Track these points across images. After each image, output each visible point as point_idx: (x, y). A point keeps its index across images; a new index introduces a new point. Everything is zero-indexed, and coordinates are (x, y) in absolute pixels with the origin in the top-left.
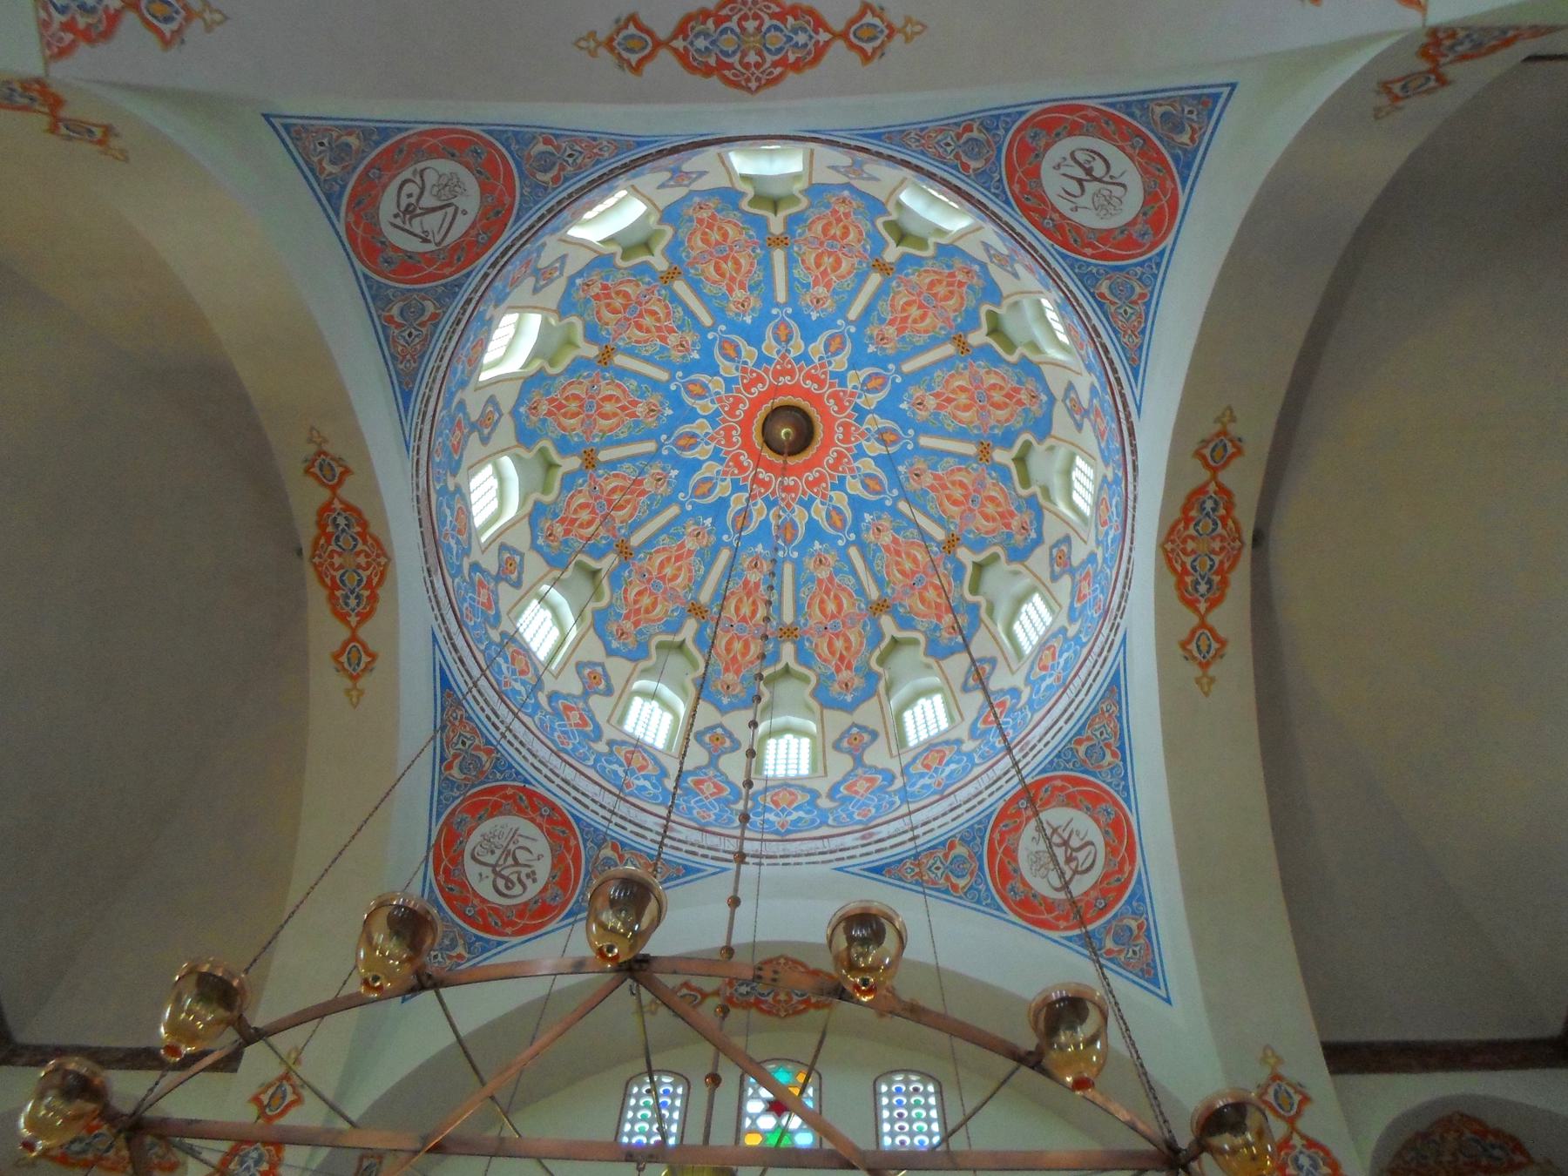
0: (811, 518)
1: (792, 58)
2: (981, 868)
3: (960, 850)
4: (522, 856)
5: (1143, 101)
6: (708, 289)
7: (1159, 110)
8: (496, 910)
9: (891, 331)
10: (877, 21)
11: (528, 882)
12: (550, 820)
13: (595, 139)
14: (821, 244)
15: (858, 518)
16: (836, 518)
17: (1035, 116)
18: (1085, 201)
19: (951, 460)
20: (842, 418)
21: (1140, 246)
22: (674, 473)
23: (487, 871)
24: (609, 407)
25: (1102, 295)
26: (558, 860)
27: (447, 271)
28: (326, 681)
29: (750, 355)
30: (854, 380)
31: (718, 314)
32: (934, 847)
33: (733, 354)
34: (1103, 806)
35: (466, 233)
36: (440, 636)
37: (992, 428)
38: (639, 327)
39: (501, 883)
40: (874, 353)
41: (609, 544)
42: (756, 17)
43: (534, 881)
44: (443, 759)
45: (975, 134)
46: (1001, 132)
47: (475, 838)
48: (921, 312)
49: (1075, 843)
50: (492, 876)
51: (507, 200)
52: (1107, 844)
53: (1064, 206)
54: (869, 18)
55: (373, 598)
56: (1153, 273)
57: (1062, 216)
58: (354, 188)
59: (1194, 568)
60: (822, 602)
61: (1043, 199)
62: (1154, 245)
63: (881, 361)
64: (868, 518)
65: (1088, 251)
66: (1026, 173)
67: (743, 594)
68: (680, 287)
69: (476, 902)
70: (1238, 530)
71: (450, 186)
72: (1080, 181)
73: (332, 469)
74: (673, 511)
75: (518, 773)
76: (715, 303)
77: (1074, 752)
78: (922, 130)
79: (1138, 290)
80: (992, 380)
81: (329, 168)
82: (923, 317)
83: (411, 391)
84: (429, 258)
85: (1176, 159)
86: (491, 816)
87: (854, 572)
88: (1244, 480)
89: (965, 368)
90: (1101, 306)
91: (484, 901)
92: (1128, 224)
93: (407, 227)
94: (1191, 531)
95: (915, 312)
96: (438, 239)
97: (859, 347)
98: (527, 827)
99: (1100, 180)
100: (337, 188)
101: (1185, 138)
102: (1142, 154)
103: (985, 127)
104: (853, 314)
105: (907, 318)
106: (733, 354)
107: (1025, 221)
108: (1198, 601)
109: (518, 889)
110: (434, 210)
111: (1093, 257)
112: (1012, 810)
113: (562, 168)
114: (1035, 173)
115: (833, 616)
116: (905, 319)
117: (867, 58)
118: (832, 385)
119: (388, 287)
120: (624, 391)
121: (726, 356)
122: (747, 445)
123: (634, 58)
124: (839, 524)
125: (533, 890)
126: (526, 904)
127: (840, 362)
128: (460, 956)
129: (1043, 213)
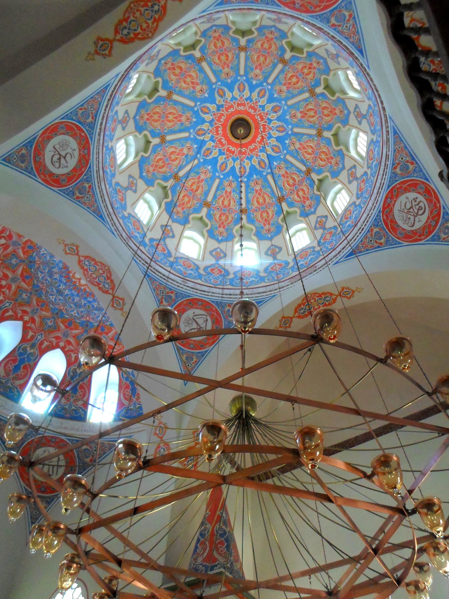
0: (267, 103)
1: (93, 263)
3: (333, 21)
4: (408, 206)
5: (25, 171)
7: (23, 165)
8: (431, 212)
9: (183, 119)
10: (67, 249)
11: (418, 201)
12: (392, 198)
13: (154, 290)
14: (168, 164)
15: (257, 86)
17: (58, 187)
18: (69, 150)
19: (214, 67)
20: (225, 113)
21: (66, 125)
23: (417, 219)
25: (93, 118)
26: (406, 190)
27: (214, 309)
28: (357, 299)
29: (221, 158)
30: (208, 117)
31: (213, 179)
32: (338, 32)
33: (224, 164)
35: (200, 309)
38: (230, 204)
39: (420, 212)
40: (195, 118)
41: (308, 179)
42: (91, 276)
43: (417, 198)
44: (379, 247)
45: (78, 194)
46: (71, 189)
47: (406, 227)
50: (419, 217)
51: (185, 303)
53: (76, 153)
54: (68, 251)
55: (323, 294)
57: (80, 150)
58: (198, 350)
59: (151, 17)
60: (294, 84)
61: (80, 161)
62: (62, 123)
63: (196, 114)
64: (254, 82)
65: (83, 134)
67: (307, 116)
68: (210, 198)
69: (429, 221)
70: (127, 10)
71: (188, 323)
72: (65, 158)
74: (289, 157)
75: (377, 216)
78: (89, 208)
79: (81, 112)
80: (173, 77)
81: (195, 360)
82: (170, 113)
84: (212, 316)
85: (31, 147)
86: (396, 222)
87: (277, 77)
88: (106, 26)
89: (176, 87)
90: (96, 116)
91: (428, 218)
92: (64, 134)
94: (139, 30)
95: (171, 117)
96: (205, 317)
97: (197, 124)
100: (200, 355)
101: (24, 151)
102: (40, 154)
103: (74, 194)
104: (186, 134)
105: (174, 118)
106: (224, 164)
107: (91, 158)
108: (162, 7)
109: (422, 204)
110: (197, 323)
111: (83, 132)
112: (303, 9)
113: (168, 293)
114: (74, 170)
115: (297, 77)
116: (176, 118)
117: (77, 247)
118: (216, 124)
120: (254, 197)
121: (226, 166)
122: (253, 141)
123: (121, 302)
124: (263, 92)
125: (421, 198)
126: (427, 200)
129: (84, 156)
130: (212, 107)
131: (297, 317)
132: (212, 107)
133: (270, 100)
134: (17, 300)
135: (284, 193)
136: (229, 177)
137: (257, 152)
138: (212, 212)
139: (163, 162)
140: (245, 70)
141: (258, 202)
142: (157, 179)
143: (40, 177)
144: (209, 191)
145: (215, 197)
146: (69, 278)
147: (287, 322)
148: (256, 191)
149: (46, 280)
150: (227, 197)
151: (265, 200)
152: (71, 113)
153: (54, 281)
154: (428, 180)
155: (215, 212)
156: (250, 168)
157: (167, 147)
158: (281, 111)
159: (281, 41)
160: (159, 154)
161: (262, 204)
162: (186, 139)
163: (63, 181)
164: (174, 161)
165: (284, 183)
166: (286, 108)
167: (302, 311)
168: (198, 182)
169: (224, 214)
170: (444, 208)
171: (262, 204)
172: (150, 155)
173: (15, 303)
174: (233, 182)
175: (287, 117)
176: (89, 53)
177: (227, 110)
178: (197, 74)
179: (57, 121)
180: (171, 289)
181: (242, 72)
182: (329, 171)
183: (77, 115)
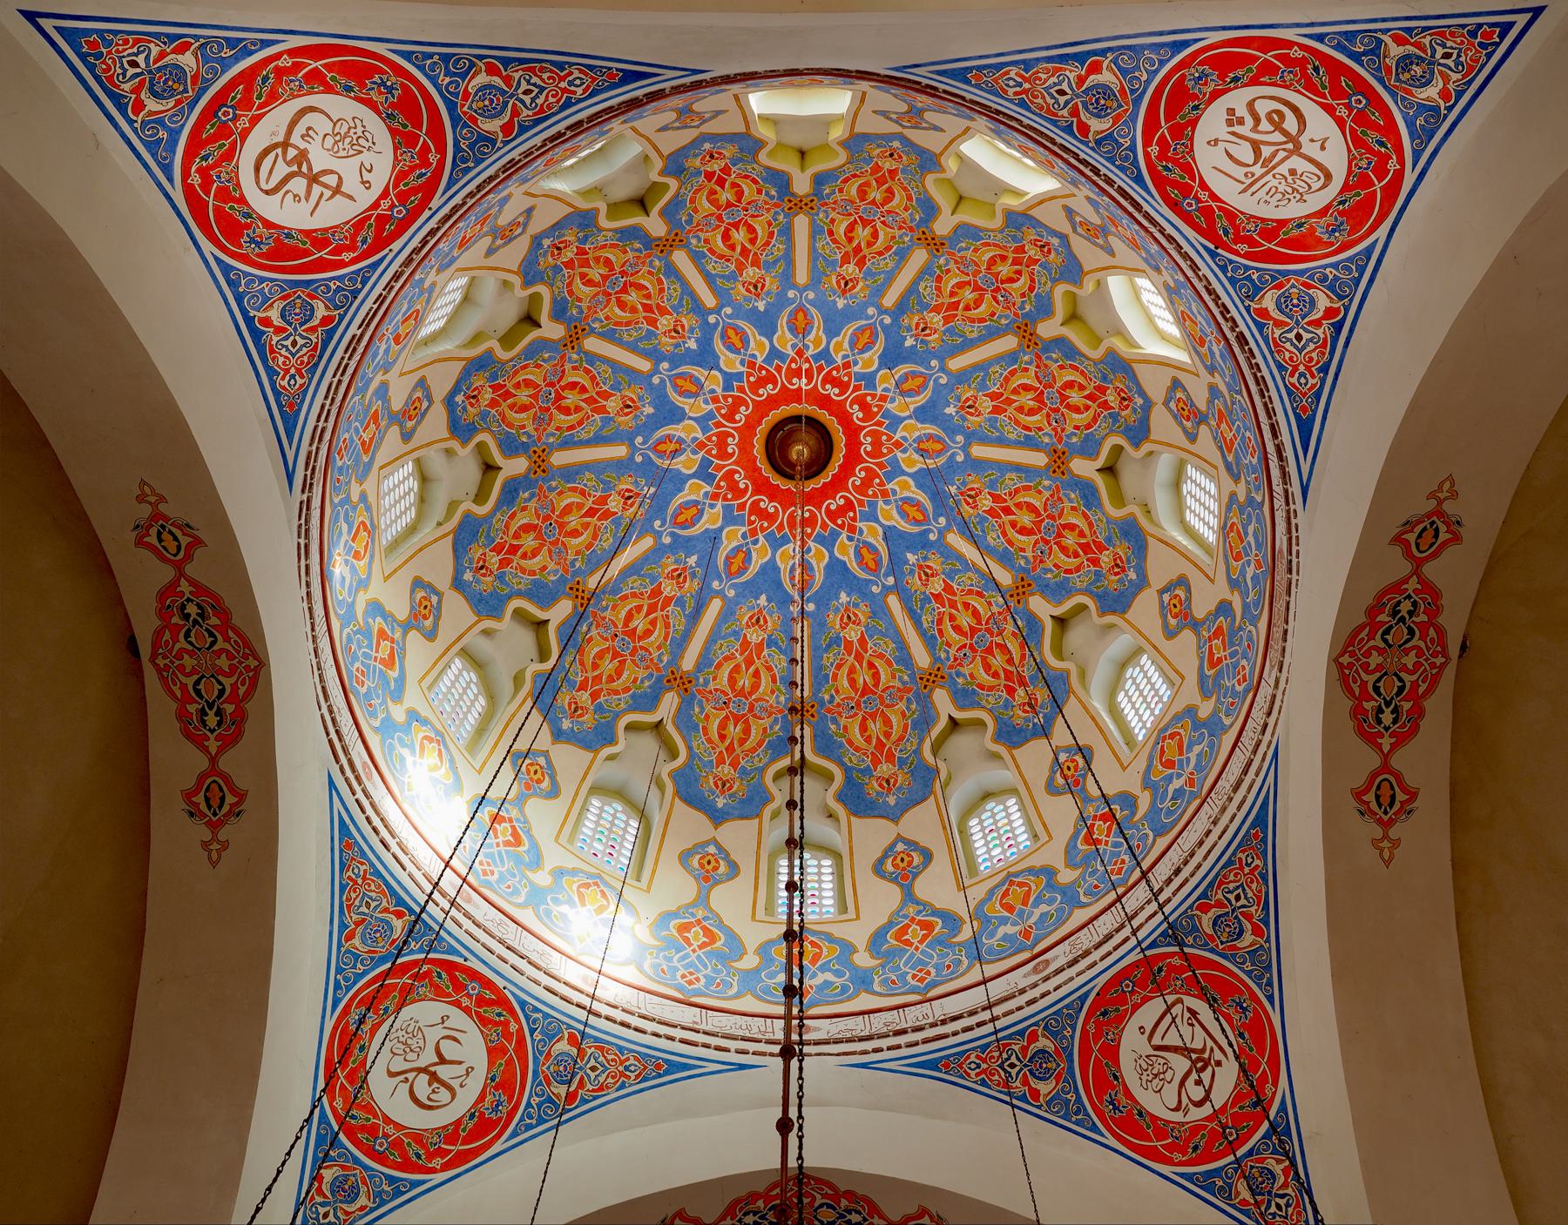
2: (451, 107)
4: (1245, 152)
5: (383, 1203)
6: (889, 648)
8: (1311, 87)
9: (668, 589)
11: (1241, 111)
16: (736, 340)
18: (433, 1035)
19: (584, 436)
22: (951, 410)
23: (1309, 149)
24: (1026, 519)
26: (1184, 131)
28: (1481, 514)
31: (879, 611)
34: (265, 249)
36: (1296, 489)
37: (532, 496)
39: (1291, 124)
41: (1046, 349)
43: (1231, 111)
44: (1338, 327)
46: (535, 1100)
47: (1316, 202)
48: (632, 625)
49: (298, 185)
50: (1303, 139)
52: (242, 200)
53: (458, 1019)
55: (1372, 612)
56: (342, 966)
57: (457, 1004)
59: (211, 634)
60: (753, 241)
63: (681, 544)
64: (692, 345)
66: (504, 1051)
67: (866, 251)
72: (442, 1061)
73: (1377, 797)
74: (956, 364)
75: (1224, 269)
76: (882, 626)
77: (331, 304)
78: (622, 1087)
83: (1252, 826)
86: (1282, 223)
87: (709, 279)
88: (175, 761)
89: (573, 563)
91: (1329, 109)
93: (1210, 1043)
97: (708, 561)
98: (1227, 191)
99: (420, 1070)
104: (715, 606)
107: (500, 983)
110: (1175, 1049)
112: (415, 199)
114: (494, 1052)
115: (736, 226)
119: (1249, 973)
124: (731, 333)
125: (1238, 99)
126: (1254, 82)
127: (732, 539)
128: (1399, 41)
129: (481, 1001)
130: (694, 491)
131: (1394, 747)
132: (694, 491)
133: (766, 325)
135: (1046, 440)
136: (906, 562)
137: (890, 438)
138: (960, 680)
139: (737, 719)
140: (645, 354)
141: (1023, 531)
142: (762, 770)
143: (433, 1171)
144: (902, 646)
145: (929, 642)
147: (1386, 792)
148: (991, 512)
150: (953, 605)
151: (1032, 508)
152: (339, 971)
154: (1185, 44)
155: (966, 671)
156: (920, 486)
157: (706, 683)
158: (813, 311)
159: (600, 230)
160: (707, 717)
161: (1038, 524)
162: (726, 614)
163: (495, 1109)
164: (755, 687)
165: (1017, 423)
166: (811, 295)
167: (1387, 717)
168: (859, 658)
169: (989, 651)
170: (1320, 38)
171: (1038, 524)
172: (690, 748)
174: (925, 558)
175: (841, 303)
176: (205, 845)
177: (723, 455)
178: (574, 490)
179: (329, 1025)
180: (1021, 1033)
181: (644, 365)
182: (1055, 281)
183: (356, 957)
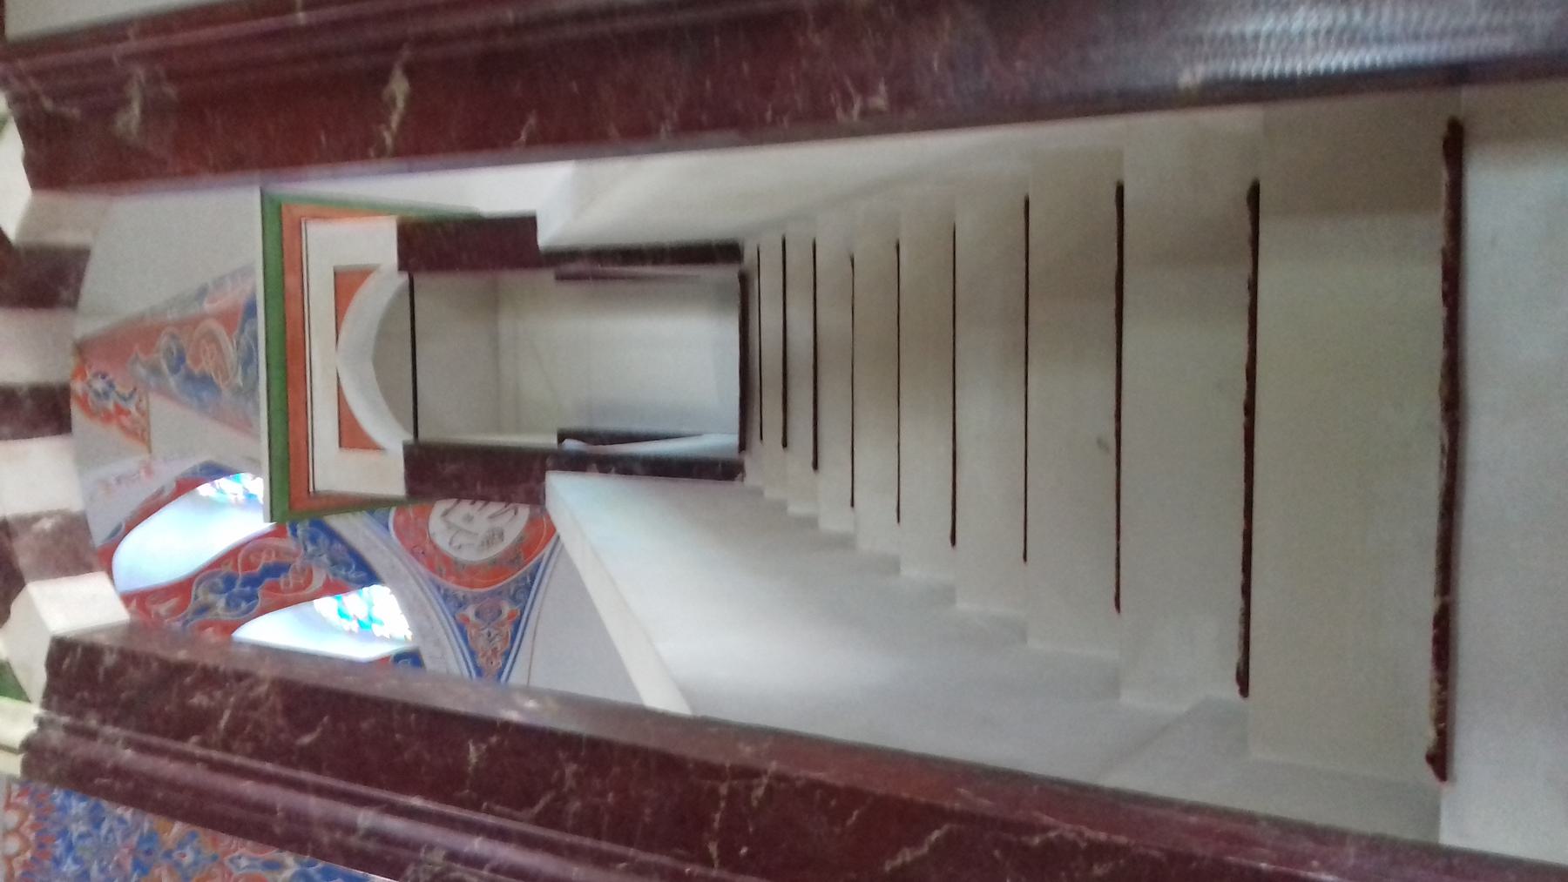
134: (214, 858)
146: (41, 846)
149: (102, 870)
153: (87, 856)
173: (225, 853)
